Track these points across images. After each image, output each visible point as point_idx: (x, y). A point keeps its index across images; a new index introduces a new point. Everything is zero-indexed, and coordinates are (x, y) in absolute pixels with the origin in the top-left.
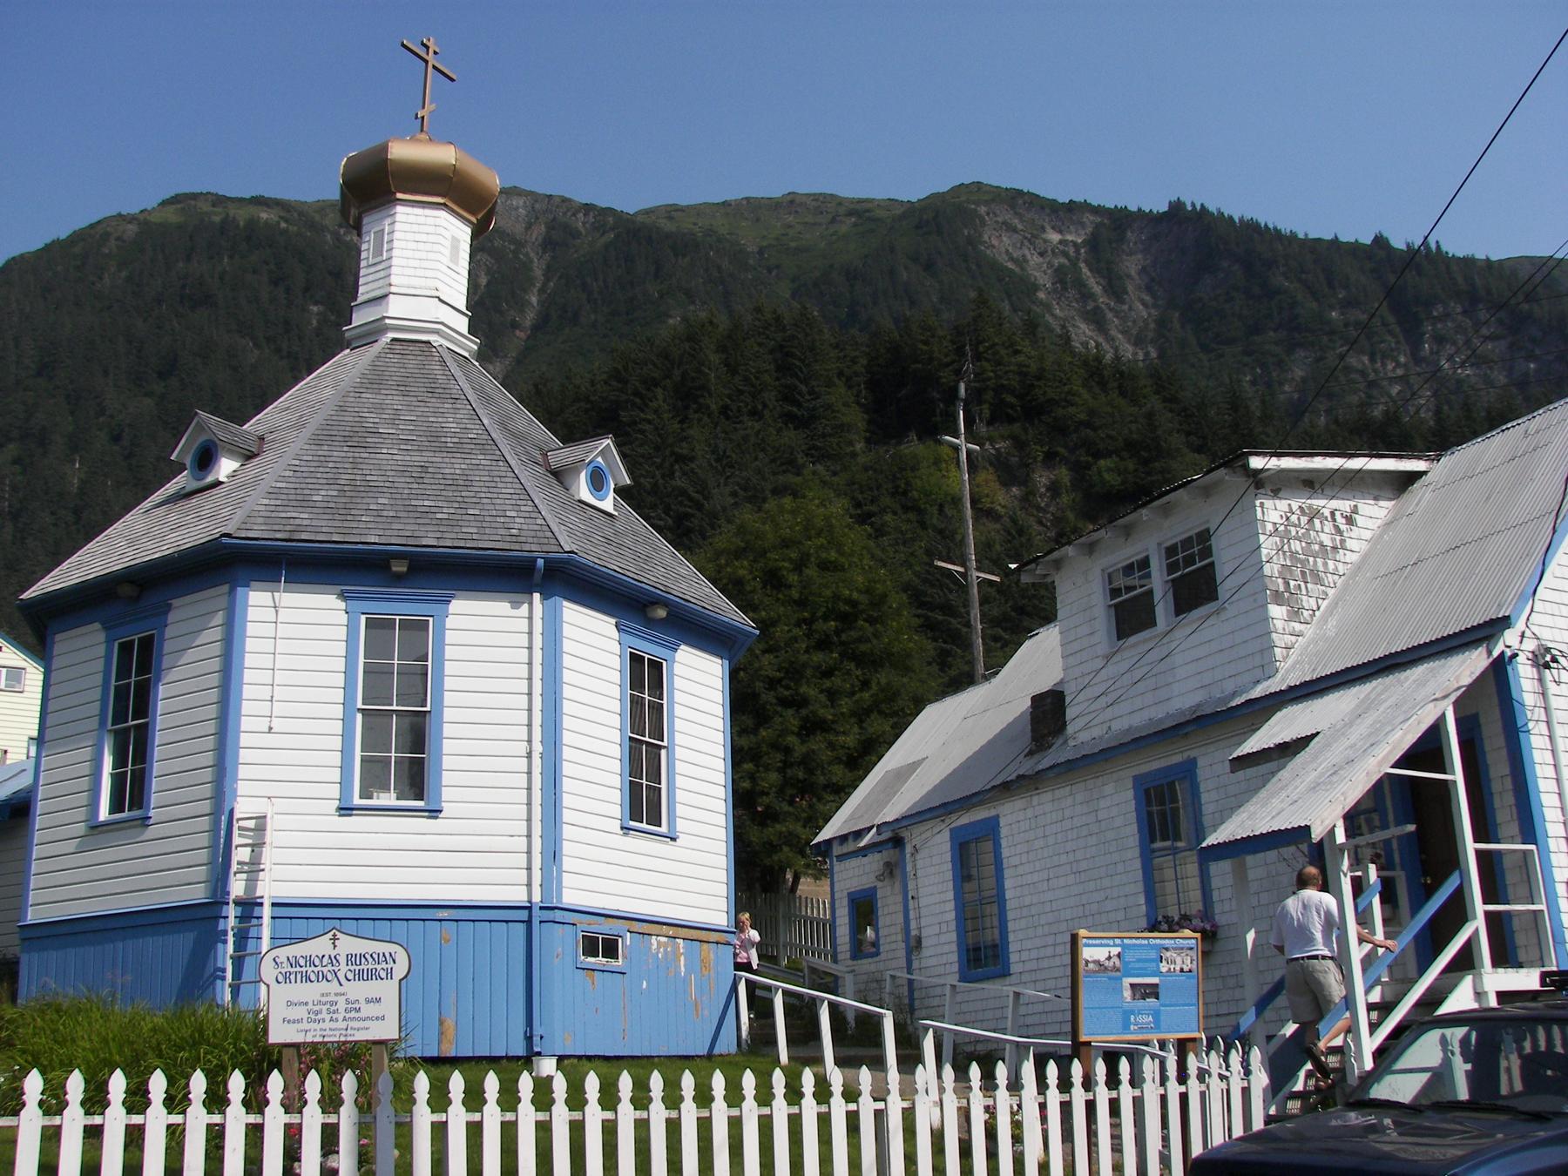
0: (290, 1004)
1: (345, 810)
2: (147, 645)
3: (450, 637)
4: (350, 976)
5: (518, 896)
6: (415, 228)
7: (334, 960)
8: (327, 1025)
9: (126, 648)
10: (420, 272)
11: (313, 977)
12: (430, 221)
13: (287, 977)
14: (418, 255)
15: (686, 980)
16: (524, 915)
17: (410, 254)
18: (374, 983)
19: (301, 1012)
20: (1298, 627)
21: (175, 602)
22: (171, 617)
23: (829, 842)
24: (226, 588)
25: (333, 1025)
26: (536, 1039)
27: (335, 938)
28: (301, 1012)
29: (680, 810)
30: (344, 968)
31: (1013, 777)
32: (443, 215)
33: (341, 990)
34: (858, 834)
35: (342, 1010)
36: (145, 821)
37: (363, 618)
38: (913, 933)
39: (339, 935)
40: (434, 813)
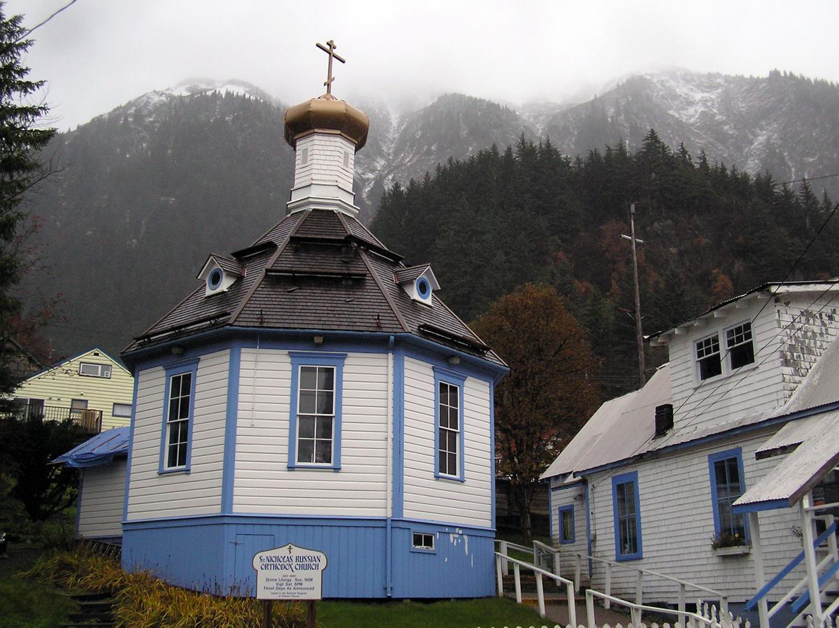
0: (267, 580)
1: (291, 468)
2: (187, 378)
3: (345, 376)
4: (298, 567)
6: (325, 148)
7: (290, 559)
8: (286, 591)
9: (176, 380)
10: (327, 172)
11: (279, 567)
12: (333, 144)
13: (266, 567)
14: (326, 163)
15: (468, 558)
17: (322, 162)
18: (309, 571)
19: (273, 584)
20: (797, 378)
21: (202, 357)
23: (549, 479)
24: (228, 351)
25: (289, 591)
26: (389, 589)
27: (290, 548)
28: (273, 584)
29: (466, 466)
30: (294, 563)
31: (645, 452)
32: (339, 139)
33: (293, 574)
34: (565, 476)
35: (293, 584)
36: (187, 471)
37: (300, 367)
38: (592, 532)
39: (292, 547)
40: (337, 470)
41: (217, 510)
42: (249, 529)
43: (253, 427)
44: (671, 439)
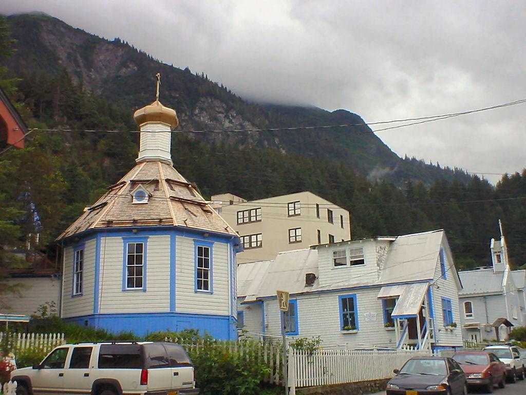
5: (226, 313)
16: (227, 318)
22: (148, 240)
24: (169, 236)
36: (145, 291)
41: (168, 310)
42: (182, 319)
43: (181, 272)
44: (314, 288)
